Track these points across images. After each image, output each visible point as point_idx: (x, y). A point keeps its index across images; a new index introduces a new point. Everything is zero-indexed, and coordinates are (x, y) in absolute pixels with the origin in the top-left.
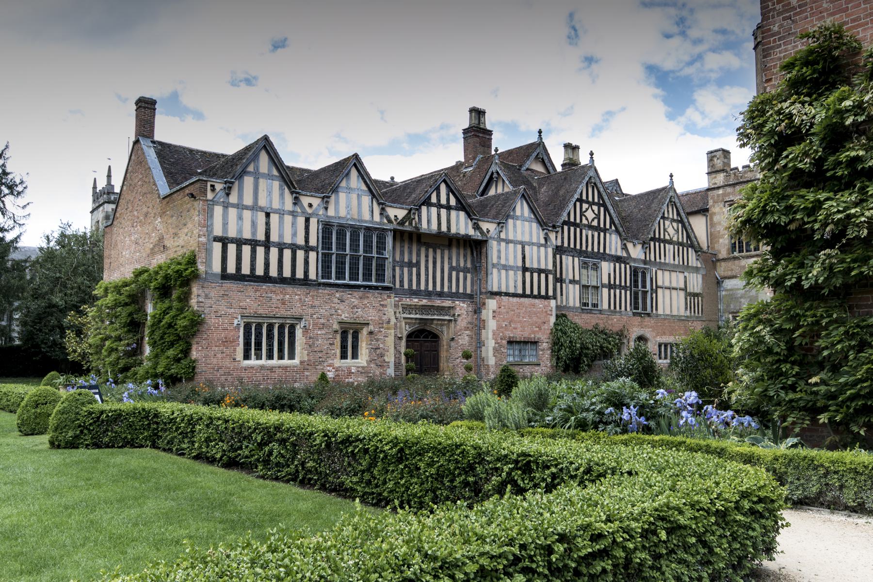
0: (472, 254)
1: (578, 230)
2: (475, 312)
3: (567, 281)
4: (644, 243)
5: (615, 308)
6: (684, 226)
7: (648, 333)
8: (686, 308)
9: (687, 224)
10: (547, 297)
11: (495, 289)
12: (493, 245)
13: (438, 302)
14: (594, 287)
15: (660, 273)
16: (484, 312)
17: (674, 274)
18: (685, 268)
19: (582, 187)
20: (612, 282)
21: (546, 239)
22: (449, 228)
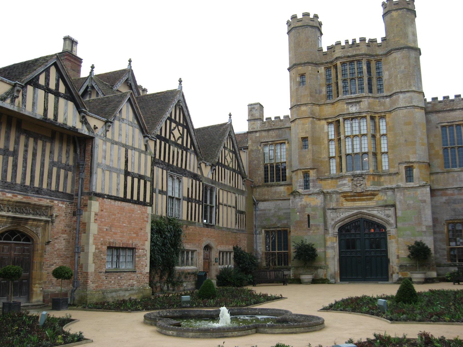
0: (75, 151)
1: (167, 145)
2: (74, 214)
3: (157, 191)
4: (212, 166)
5: (191, 219)
6: (236, 157)
7: (213, 244)
8: (236, 223)
9: (238, 155)
10: (144, 204)
11: (99, 191)
12: (98, 142)
13: (35, 200)
14: (177, 199)
15: (221, 191)
16: (85, 214)
17: (229, 194)
18: (235, 190)
19: (171, 109)
20: (190, 196)
21: (146, 146)
22: (56, 116)
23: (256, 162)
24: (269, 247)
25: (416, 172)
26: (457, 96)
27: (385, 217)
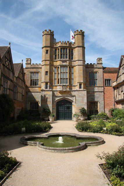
23: (28, 78)
24: (31, 108)
25: (82, 86)
26: (94, 64)
27: (72, 99)
